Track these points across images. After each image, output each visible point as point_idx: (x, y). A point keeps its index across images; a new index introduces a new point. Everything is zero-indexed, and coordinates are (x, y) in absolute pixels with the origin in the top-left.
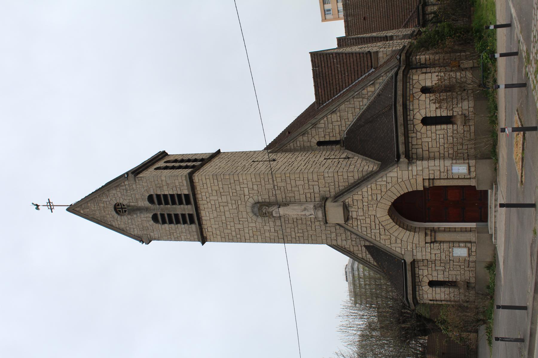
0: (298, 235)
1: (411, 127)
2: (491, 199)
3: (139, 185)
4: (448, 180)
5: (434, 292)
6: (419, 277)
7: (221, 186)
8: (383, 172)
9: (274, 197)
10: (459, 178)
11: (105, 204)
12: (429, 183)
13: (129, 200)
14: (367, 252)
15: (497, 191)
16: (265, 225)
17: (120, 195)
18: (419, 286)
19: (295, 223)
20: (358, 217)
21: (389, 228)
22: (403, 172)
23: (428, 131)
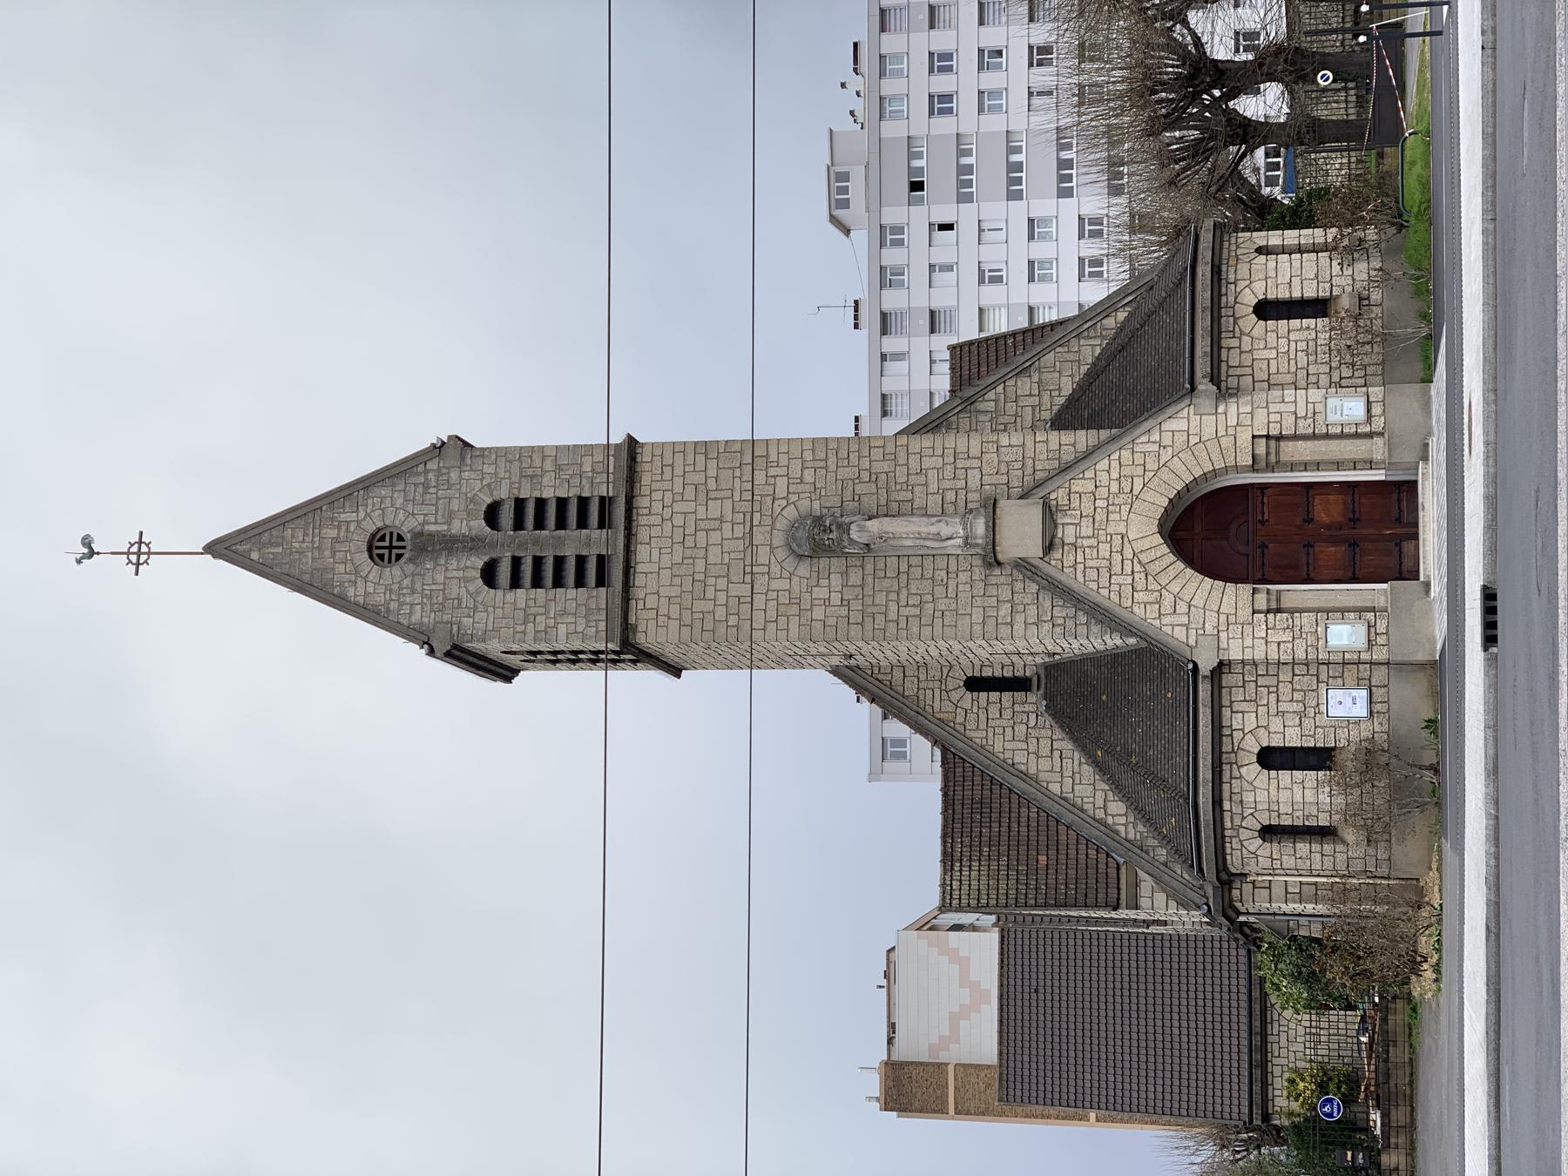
0: (905, 611)
1: (1228, 322)
3: (471, 470)
4: (1316, 442)
5: (1274, 783)
6: (1231, 735)
7: (712, 472)
9: (856, 504)
10: (1342, 436)
11: (344, 528)
12: (1268, 447)
13: (425, 515)
14: (1083, 760)
16: (817, 586)
17: (399, 502)
18: (1231, 764)
19: (904, 577)
20: (1079, 540)
23: (1269, 334)
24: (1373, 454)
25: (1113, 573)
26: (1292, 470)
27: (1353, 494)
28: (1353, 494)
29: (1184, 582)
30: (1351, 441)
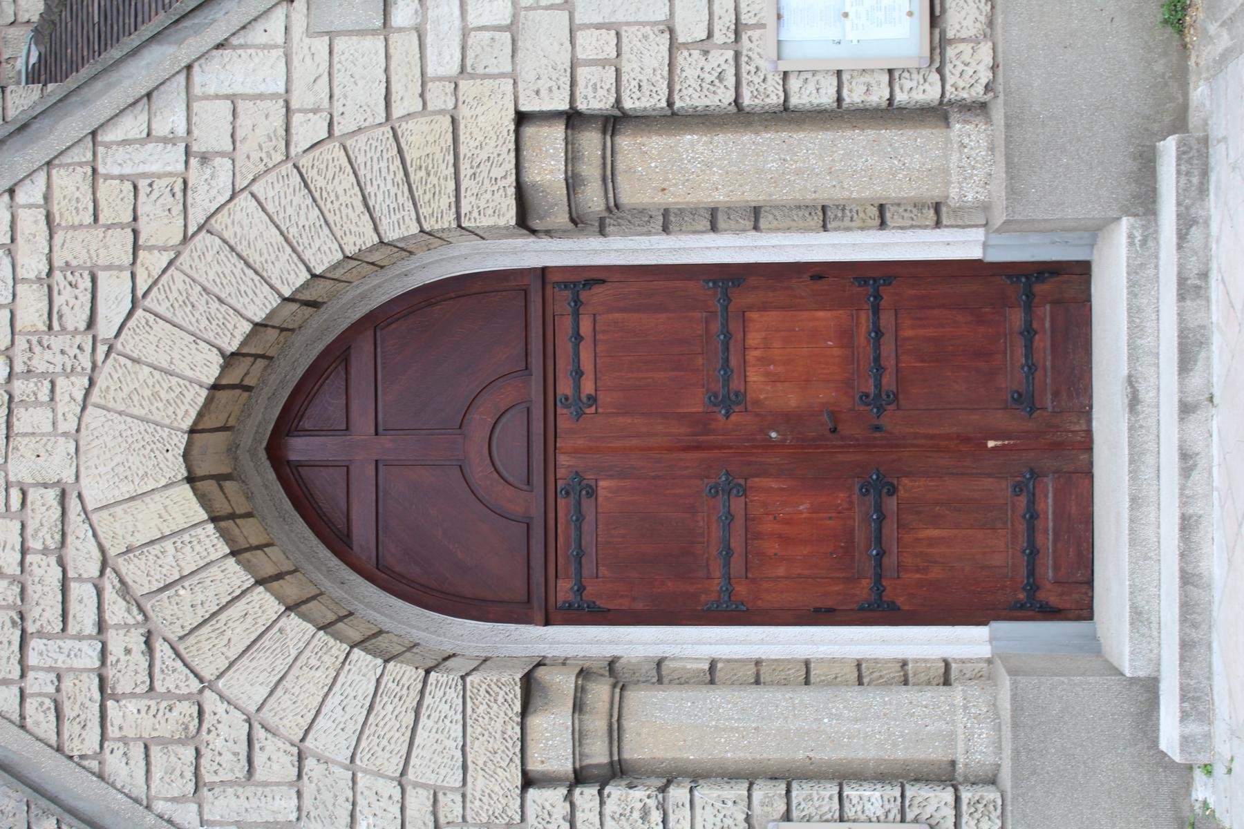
2: (1134, 311)
4: (747, 138)
8: (155, 53)
12: (572, 156)
15: (1203, 190)
21: (191, 620)
22: (341, 44)
24: (948, 183)
25: (31, 628)
26: (666, 229)
27: (876, 310)
28: (876, 310)
29: (281, 667)
30: (871, 133)
